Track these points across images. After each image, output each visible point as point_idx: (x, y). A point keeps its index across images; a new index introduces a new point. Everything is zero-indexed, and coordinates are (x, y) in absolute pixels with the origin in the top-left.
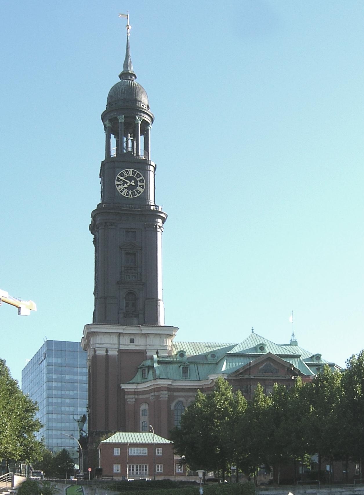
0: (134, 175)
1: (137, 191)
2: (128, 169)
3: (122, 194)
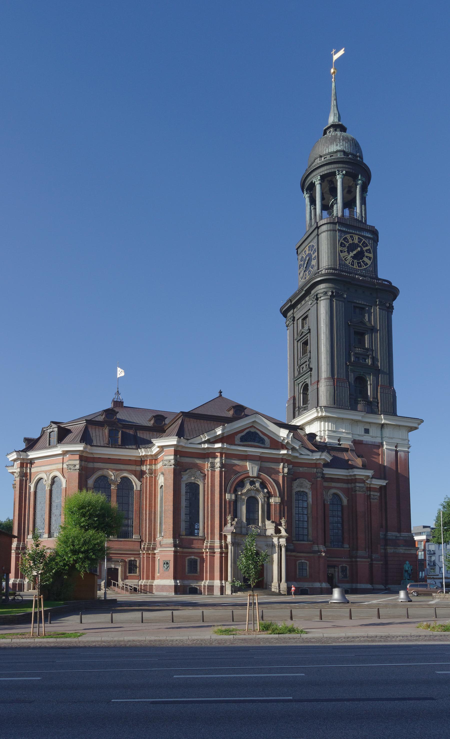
0: (360, 243)
1: (363, 262)
2: (354, 235)
3: (347, 262)
